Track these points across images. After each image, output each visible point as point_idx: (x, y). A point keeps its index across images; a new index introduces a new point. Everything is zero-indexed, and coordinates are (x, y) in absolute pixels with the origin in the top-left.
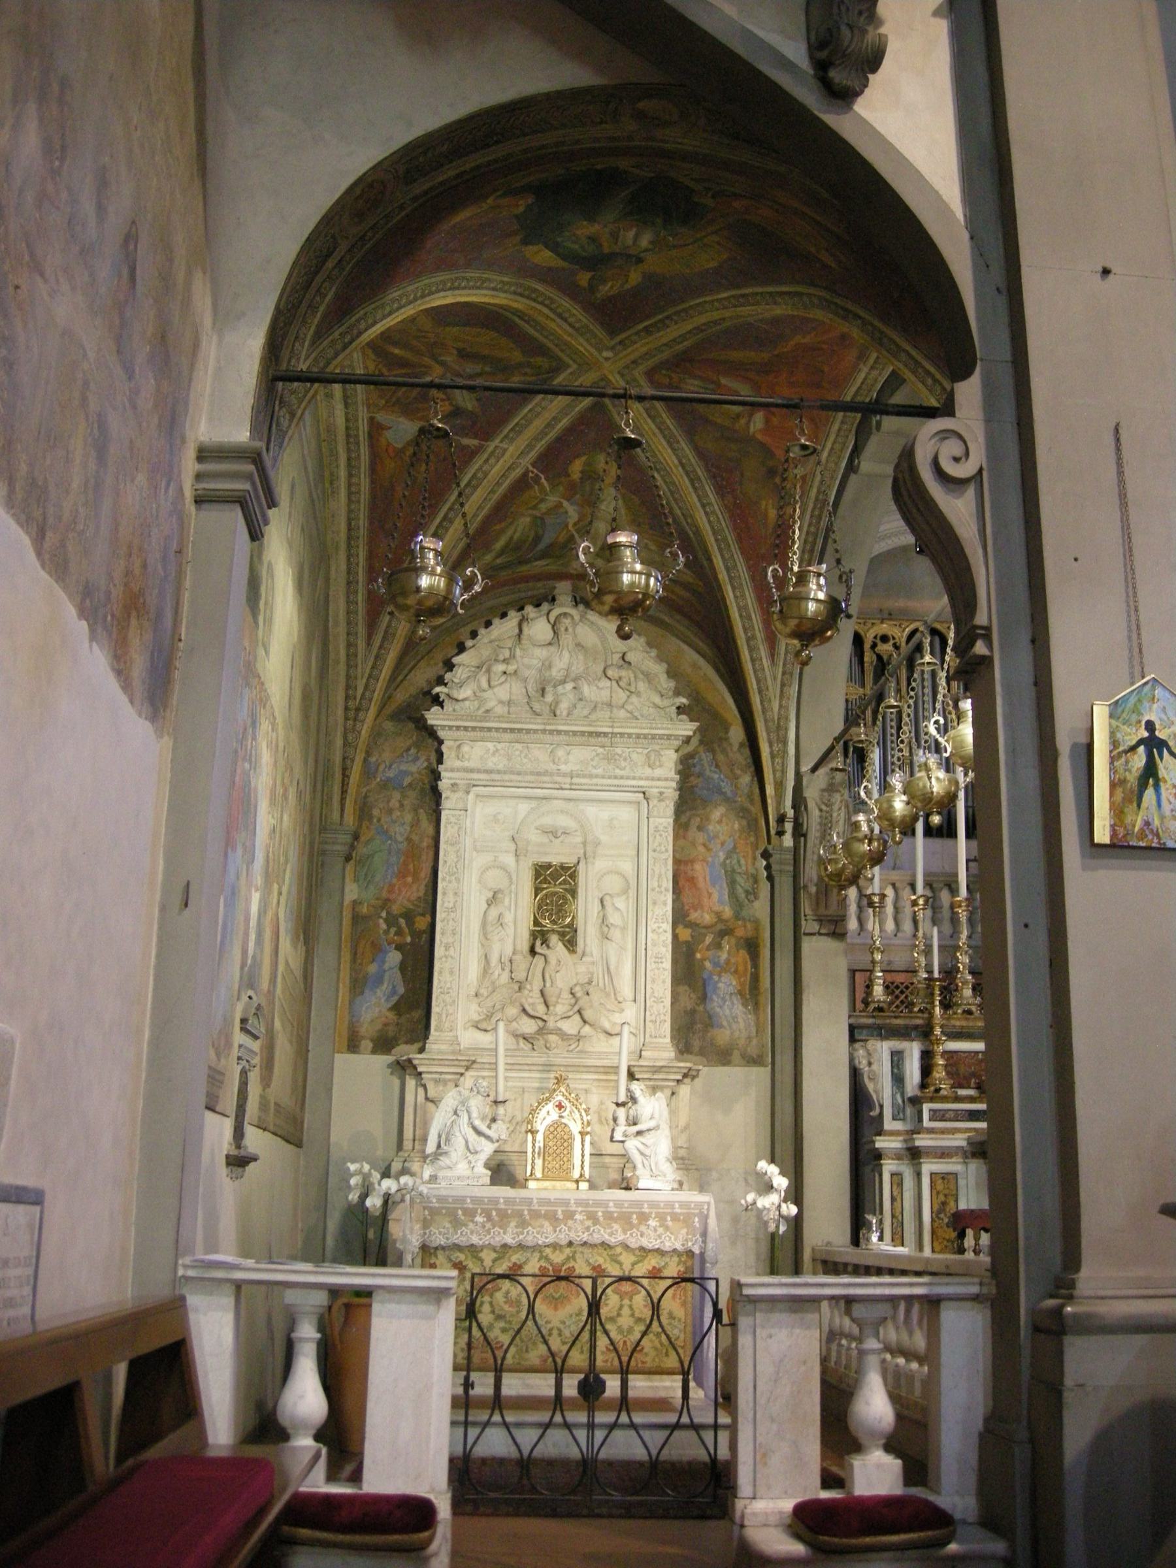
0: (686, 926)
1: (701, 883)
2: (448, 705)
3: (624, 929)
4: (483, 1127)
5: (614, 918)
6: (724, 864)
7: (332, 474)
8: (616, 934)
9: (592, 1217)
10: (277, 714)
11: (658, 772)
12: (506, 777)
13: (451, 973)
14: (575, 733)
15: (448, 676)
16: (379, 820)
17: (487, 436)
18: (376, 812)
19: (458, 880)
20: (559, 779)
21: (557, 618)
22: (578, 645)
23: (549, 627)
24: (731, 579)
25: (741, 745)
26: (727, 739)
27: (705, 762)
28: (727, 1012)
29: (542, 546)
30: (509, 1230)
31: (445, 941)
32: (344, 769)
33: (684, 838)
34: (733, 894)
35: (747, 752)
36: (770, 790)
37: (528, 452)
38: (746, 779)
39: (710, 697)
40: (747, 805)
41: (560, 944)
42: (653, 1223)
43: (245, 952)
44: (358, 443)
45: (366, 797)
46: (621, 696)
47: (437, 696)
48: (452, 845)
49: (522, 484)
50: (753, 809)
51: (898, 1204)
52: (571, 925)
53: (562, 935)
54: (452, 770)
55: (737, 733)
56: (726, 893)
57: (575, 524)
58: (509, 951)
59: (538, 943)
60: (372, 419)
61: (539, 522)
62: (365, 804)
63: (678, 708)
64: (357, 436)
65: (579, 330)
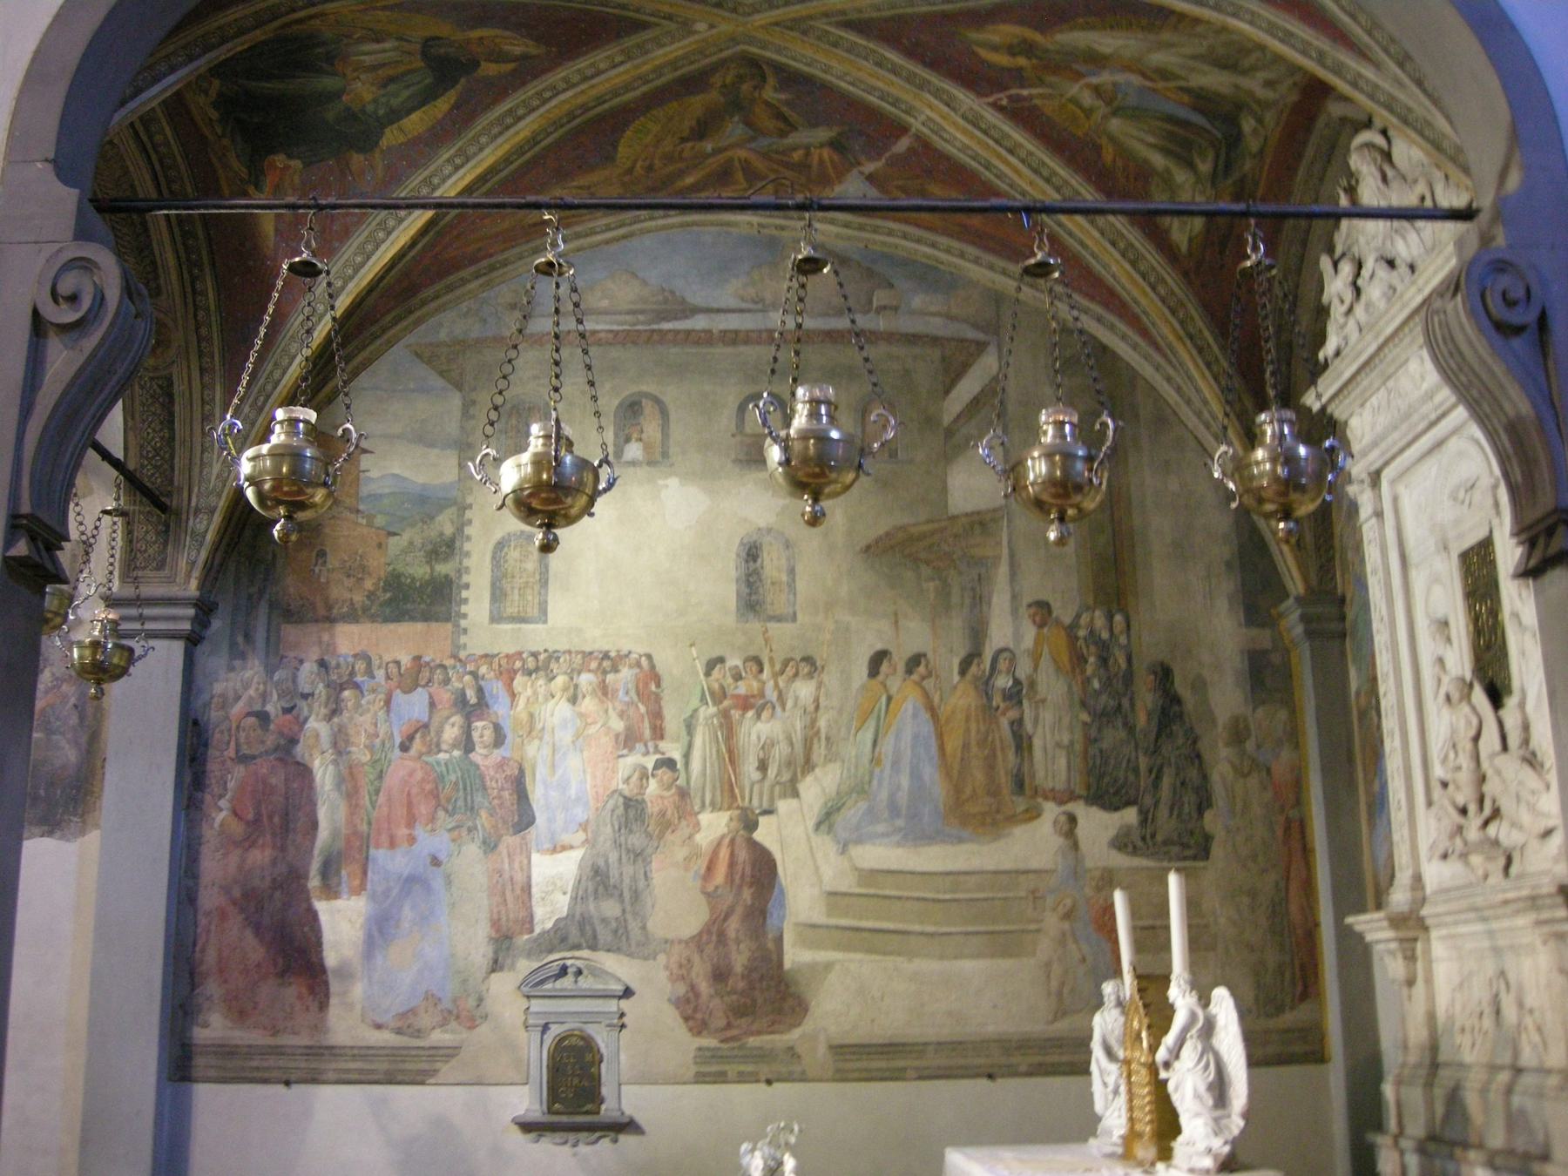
17: (903, 129)
57: (1151, 80)
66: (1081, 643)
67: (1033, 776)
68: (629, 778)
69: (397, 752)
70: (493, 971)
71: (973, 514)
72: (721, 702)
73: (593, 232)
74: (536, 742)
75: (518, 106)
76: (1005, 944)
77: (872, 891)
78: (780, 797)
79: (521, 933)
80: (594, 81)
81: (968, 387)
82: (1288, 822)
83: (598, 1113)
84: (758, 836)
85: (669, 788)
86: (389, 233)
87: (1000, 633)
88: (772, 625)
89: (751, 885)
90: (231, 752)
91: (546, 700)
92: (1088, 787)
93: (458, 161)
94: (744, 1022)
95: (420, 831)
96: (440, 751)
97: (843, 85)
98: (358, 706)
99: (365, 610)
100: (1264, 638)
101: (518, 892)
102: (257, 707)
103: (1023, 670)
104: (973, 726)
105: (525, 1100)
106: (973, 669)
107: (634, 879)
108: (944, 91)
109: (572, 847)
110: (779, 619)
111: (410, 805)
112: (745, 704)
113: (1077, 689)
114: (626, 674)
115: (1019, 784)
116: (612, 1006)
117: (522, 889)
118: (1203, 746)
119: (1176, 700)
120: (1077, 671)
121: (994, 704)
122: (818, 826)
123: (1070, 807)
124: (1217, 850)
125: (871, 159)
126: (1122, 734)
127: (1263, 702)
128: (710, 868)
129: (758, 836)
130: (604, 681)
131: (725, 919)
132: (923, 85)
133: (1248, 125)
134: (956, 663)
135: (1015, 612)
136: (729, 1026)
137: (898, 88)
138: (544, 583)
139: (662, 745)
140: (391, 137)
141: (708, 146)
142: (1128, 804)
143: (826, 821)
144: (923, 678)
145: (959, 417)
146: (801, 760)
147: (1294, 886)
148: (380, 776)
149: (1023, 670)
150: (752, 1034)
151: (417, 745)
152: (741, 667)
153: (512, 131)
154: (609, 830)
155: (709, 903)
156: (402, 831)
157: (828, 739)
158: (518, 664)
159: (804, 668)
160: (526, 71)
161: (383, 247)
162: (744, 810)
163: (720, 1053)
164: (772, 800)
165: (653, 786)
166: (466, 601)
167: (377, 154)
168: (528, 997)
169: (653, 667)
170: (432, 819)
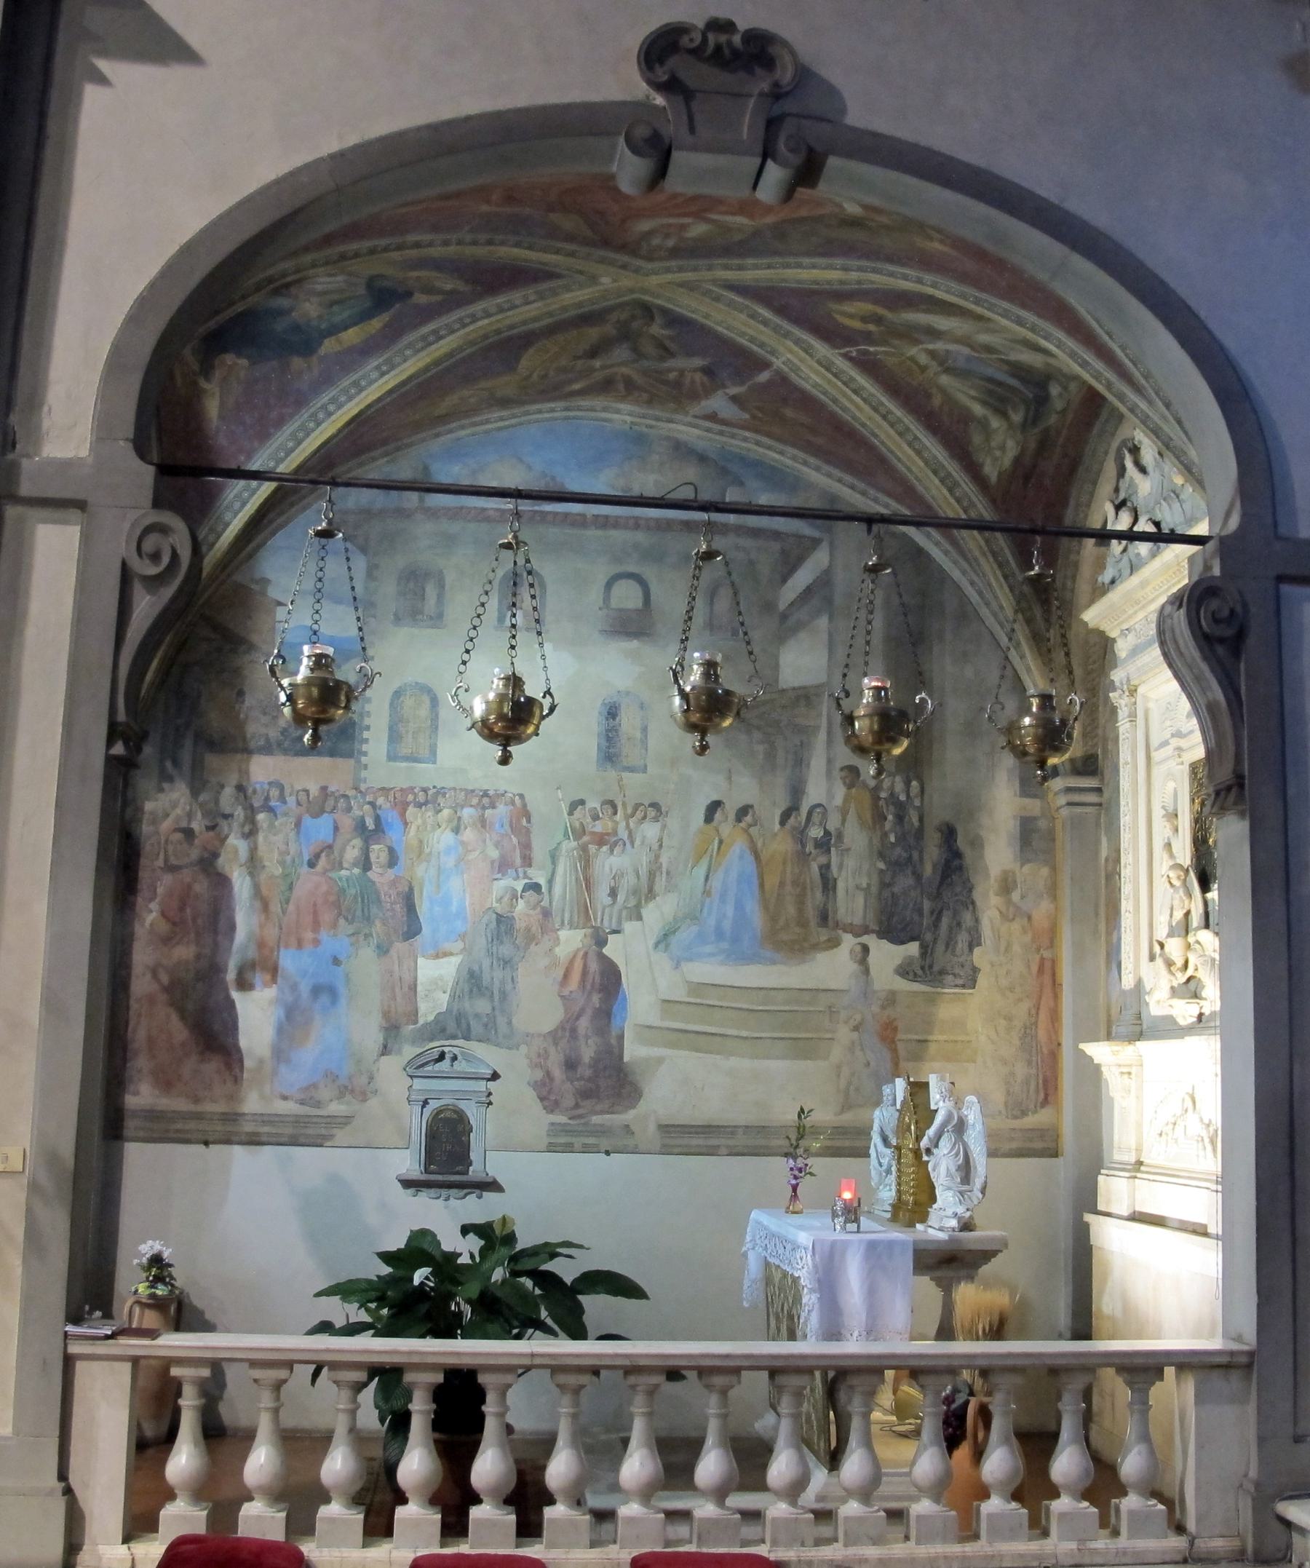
17: (766, 365)
37: (811, 347)
57: (978, 352)
60: (695, 417)
66: (882, 803)
67: (835, 912)
68: (501, 898)
69: (305, 869)
70: (383, 1054)
71: (800, 688)
72: (581, 838)
73: (488, 421)
74: (425, 864)
75: (440, 328)
76: (804, 1048)
77: (698, 1001)
78: (627, 920)
79: (407, 1024)
80: (510, 313)
81: (803, 577)
82: (1042, 959)
83: (466, 1173)
84: (605, 951)
85: (534, 908)
86: (318, 424)
87: (815, 792)
88: (625, 775)
89: (600, 991)
90: (160, 862)
91: (434, 830)
92: (880, 923)
93: (384, 368)
94: (587, 1104)
95: (324, 935)
96: (342, 868)
97: (720, 329)
98: (271, 826)
99: (279, 744)
100: (1034, 806)
101: (406, 989)
102: (184, 824)
103: (833, 824)
104: (789, 870)
105: (408, 1162)
106: (792, 821)
107: (503, 982)
108: (804, 341)
109: (451, 954)
110: (631, 769)
111: (315, 913)
112: (601, 840)
113: (876, 841)
114: (502, 810)
115: (824, 918)
116: (482, 1086)
117: (410, 988)
118: (977, 895)
119: (958, 855)
120: (878, 827)
121: (807, 850)
122: (657, 945)
123: (865, 939)
124: (982, 980)
126: (910, 881)
127: (1029, 861)
128: (566, 976)
129: (605, 951)
130: (483, 815)
131: (578, 1018)
132: (787, 335)
133: (1054, 390)
134: (777, 814)
135: (829, 773)
136: (577, 1106)
137: (766, 335)
138: (434, 728)
139: (530, 871)
140: (329, 346)
141: (597, 363)
142: (913, 939)
143: (664, 940)
144: (750, 826)
145: (792, 604)
146: (645, 890)
147: (1043, 1016)
148: (291, 888)
149: (833, 824)
150: (597, 1113)
151: (322, 862)
152: (599, 809)
153: (434, 347)
154: (483, 941)
155: (564, 1005)
156: (309, 935)
157: (668, 873)
158: (410, 797)
159: (652, 813)
160: (453, 301)
161: (313, 435)
162: (596, 929)
163: (568, 1128)
164: (619, 922)
165: (521, 905)
166: (366, 741)
167: (314, 359)
168: (411, 1077)
169: (525, 805)
170: (334, 925)
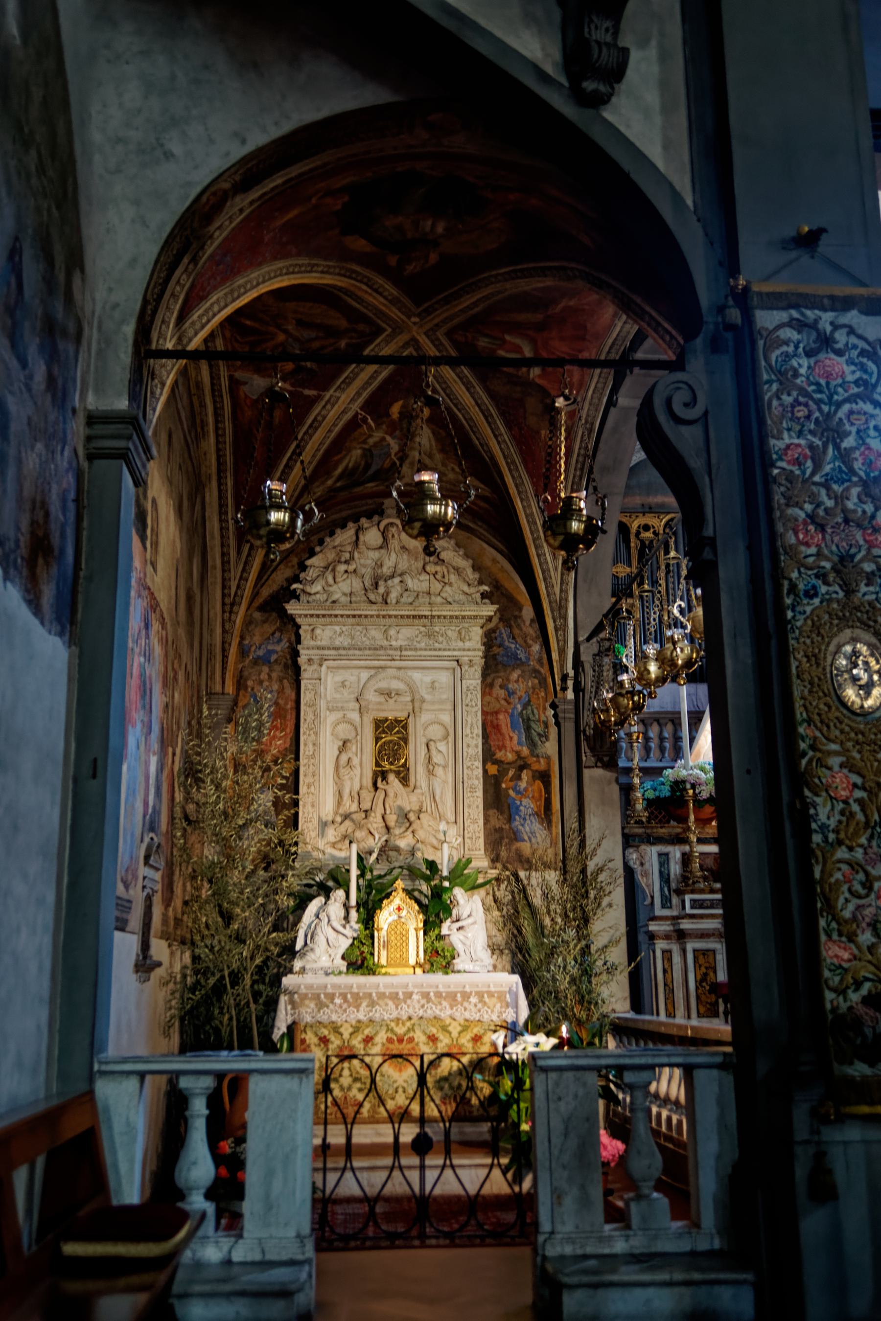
0: (493, 763)
1: (504, 729)
2: (303, 598)
3: (445, 767)
4: (341, 929)
5: (437, 759)
6: (521, 714)
7: (202, 421)
8: (439, 771)
9: (426, 995)
10: (166, 615)
11: (468, 644)
12: (351, 652)
13: (313, 806)
14: (402, 617)
15: (302, 575)
16: (252, 689)
18: (250, 683)
19: (316, 734)
20: (391, 652)
21: (387, 526)
22: (403, 548)
23: (379, 534)
24: (519, 493)
25: (532, 621)
26: (520, 617)
27: (504, 636)
28: (527, 829)
29: (371, 472)
30: (361, 1009)
31: (307, 781)
32: (224, 650)
33: (490, 694)
34: (529, 737)
35: (536, 626)
36: (555, 656)
38: (536, 648)
39: (507, 584)
40: (538, 667)
41: (397, 781)
42: (474, 1000)
43: (146, 804)
44: (222, 397)
45: (241, 671)
46: (437, 586)
47: (295, 590)
48: (310, 706)
49: (354, 424)
50: (542, 671)
51: (669, 975)
52: (404, 765)
53: (397, 773)
54: (308, 649)
55: (528, 612)
56: (524, 736)
57: (396, 454)
58: (357, 787)
59: (379, 780)
61: (368, 454)
62: (241, 677)
63: (482, 594)
64: (220, 391)
65: (394, 301)
125: (292, 385)
